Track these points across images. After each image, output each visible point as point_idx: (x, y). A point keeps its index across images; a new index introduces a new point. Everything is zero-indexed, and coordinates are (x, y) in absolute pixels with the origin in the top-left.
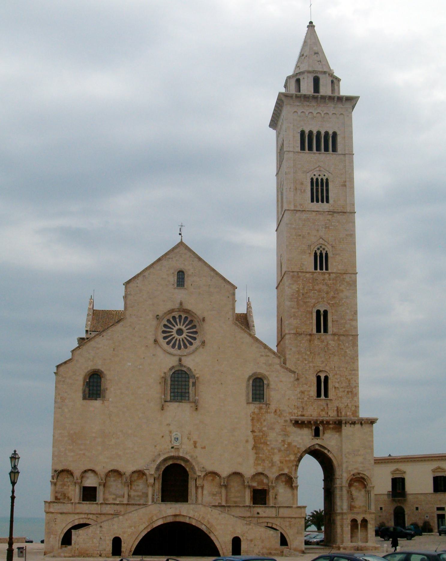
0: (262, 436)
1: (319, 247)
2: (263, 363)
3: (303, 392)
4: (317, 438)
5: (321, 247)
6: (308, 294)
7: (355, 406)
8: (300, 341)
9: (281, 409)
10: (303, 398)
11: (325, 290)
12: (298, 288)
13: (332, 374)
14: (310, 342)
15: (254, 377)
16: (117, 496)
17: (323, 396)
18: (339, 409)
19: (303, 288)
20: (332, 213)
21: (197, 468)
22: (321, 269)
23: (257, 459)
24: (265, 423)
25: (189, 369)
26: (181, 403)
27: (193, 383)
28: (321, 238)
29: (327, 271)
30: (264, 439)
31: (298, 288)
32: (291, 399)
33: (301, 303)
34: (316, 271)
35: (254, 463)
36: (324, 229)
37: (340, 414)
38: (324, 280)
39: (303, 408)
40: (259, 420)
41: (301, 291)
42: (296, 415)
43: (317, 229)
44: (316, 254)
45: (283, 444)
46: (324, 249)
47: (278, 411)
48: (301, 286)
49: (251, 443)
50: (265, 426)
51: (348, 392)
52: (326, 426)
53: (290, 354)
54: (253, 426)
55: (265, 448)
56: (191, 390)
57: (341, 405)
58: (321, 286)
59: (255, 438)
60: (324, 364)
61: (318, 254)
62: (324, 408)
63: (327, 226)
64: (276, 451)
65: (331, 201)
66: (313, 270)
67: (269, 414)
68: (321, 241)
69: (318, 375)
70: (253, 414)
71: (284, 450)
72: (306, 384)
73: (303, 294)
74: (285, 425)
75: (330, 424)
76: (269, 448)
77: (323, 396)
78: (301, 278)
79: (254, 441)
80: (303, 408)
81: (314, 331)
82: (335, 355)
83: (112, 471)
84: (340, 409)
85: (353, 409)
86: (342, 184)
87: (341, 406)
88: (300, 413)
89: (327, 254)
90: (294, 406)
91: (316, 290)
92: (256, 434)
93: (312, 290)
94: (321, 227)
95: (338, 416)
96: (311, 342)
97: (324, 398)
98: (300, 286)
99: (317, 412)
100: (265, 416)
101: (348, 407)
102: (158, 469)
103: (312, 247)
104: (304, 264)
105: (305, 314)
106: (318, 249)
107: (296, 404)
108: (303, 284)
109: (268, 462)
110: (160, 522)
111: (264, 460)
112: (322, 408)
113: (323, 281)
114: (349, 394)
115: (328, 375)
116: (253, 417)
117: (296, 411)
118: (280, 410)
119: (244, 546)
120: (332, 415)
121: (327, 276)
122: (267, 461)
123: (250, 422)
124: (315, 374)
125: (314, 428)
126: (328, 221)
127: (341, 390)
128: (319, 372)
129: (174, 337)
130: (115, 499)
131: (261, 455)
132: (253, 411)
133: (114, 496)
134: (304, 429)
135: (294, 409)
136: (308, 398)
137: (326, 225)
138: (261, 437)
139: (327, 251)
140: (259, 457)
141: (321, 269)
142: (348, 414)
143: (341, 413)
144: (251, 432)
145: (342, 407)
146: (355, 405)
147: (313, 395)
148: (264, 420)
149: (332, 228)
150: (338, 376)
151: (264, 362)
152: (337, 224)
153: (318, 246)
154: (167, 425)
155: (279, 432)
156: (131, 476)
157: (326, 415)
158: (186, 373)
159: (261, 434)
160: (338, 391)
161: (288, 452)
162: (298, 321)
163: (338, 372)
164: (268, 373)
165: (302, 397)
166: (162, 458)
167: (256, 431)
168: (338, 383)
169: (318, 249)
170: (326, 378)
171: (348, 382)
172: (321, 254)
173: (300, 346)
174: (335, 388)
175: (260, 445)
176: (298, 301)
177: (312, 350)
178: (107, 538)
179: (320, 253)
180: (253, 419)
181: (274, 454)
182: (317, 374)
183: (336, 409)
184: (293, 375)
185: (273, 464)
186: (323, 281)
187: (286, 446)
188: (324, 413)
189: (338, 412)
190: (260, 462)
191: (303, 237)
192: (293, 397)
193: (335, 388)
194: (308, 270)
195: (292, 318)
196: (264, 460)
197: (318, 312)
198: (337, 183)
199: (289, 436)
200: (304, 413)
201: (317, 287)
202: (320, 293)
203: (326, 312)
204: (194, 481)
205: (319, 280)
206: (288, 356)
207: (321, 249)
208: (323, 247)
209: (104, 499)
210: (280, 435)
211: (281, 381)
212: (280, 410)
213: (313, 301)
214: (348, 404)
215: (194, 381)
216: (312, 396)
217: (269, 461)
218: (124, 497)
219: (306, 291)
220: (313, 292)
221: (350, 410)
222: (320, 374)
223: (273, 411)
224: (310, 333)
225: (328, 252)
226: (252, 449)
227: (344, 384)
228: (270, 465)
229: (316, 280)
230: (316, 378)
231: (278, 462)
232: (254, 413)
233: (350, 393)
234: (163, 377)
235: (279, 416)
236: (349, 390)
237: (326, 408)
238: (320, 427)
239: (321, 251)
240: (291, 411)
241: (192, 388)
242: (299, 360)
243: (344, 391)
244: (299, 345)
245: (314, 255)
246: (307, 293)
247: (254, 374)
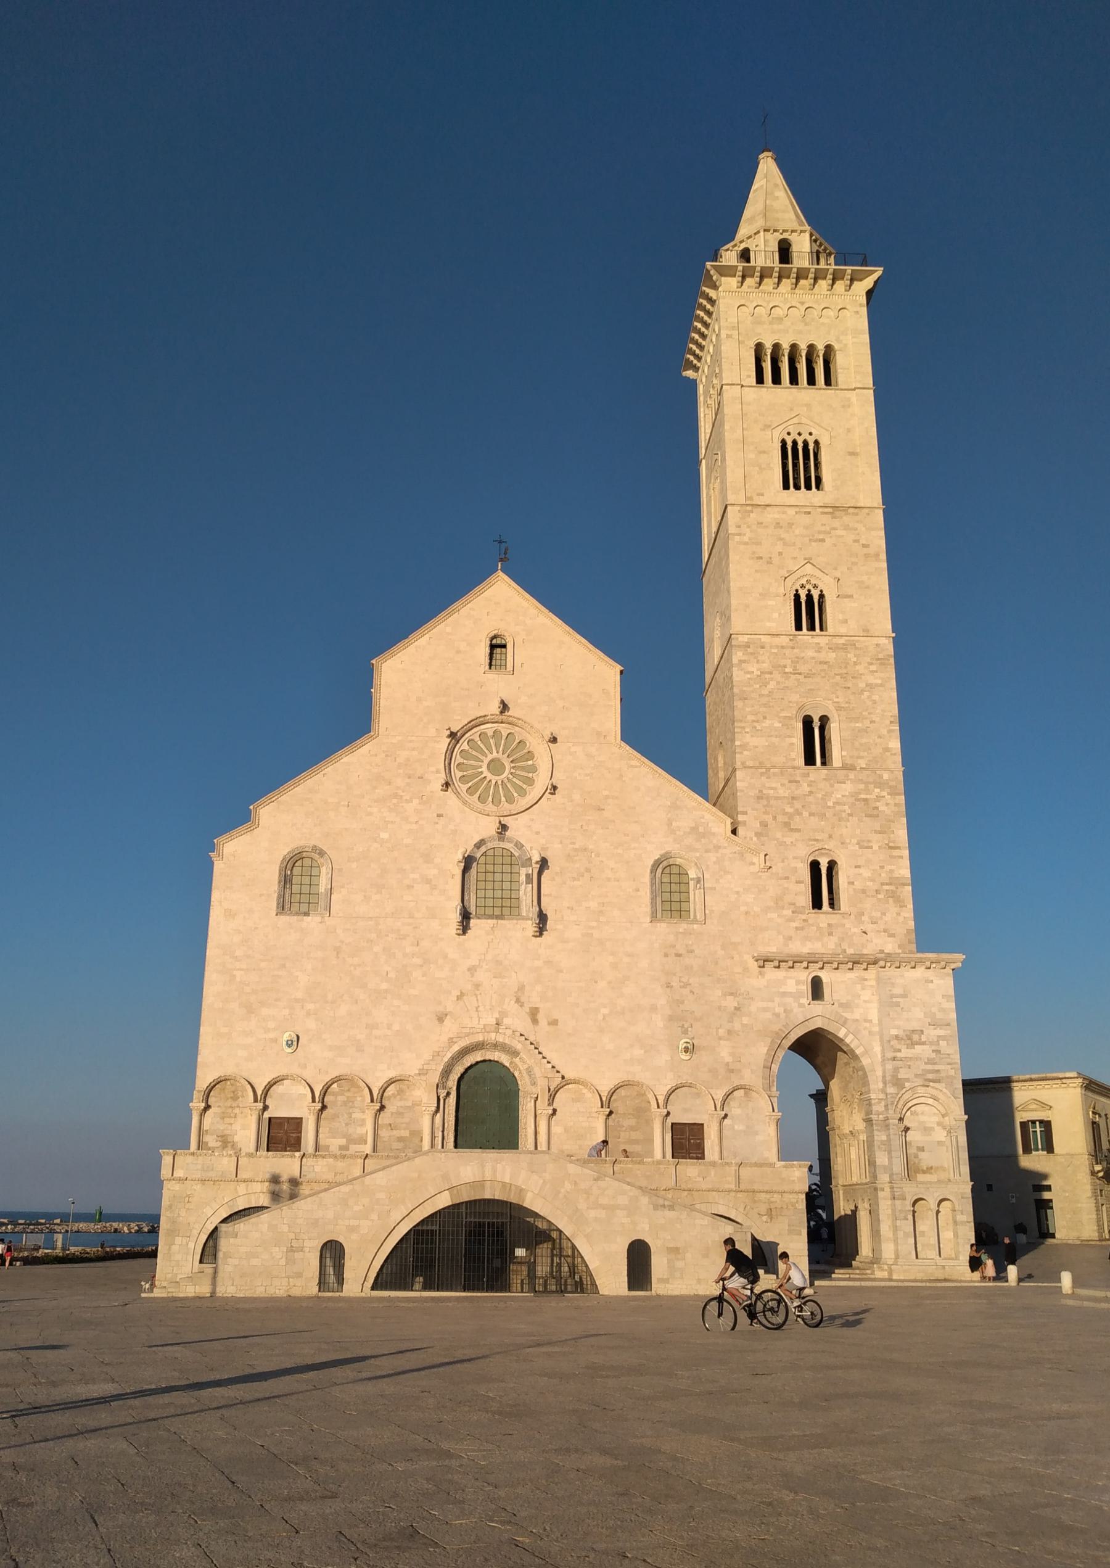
1: (805, 582)
5: (808, 582)
15: (665, 864)
16: (351, 1141)
20: (830, 510)
21: (538, 1072)
22: (812, 628)
25: (519, 846)
26: (500, 921)
27: (528, 876)
29: (822, 633)
34: (800, 633)
44: (797, 597)
46: (815, 586)
56: (526, 893)
61: (803, 599)
81: (801, 760)
83: (337, 1080)
89: (822, 596)
102: (446, 1072)
103: (789, 582)
106: (803, 586)
110: (444, 1201)
119: (658, 1265)
129: (485, 777)
130: (341, 1148)
133: (343, 1142)
139: (821, 591)
141: (812, 628)
153: (804, 581)
154: (469, 970)
156: (384, 1090)
158: (512, 855)
166: (456, 1048)
169: (801, 587)
172: (809, 596)
178: (307, 1244)
184: (755, 860)
191: (770, 562)
204: (533, 1101)
206: (740, 818)
207: (808, 587)
208: (813, 582)
209: (317, 1148)
215: (530, 872)
218: (366, 1143)
225: (824, 593)
234: (460, 862)
239: (809, 591)
241: (526, 888)
245: (794, 600)
247: (666, 856)
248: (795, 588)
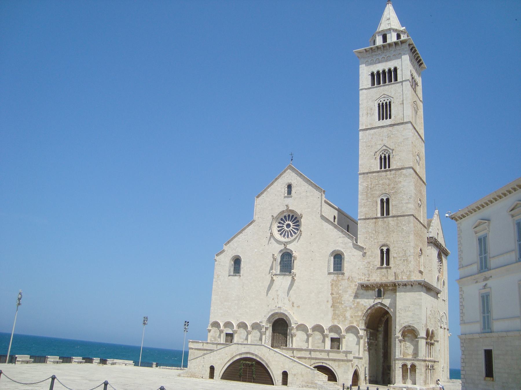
0: (339, 297)
2: (341, 243)
3: (369, 263)
4: (379, 298)
6: (374, 188)
7: (410, 271)
8: (368, 224)
9: (352, 276)
10: (369, 267)
11: (387, 183)
12: (367, 184)
13: (392, 247)
14: (375, 223)
17: (385, 265)
18: (397, 274)
19: (371, 184)
22: (385, 167)
23: (334, 314)
24: (341, 288)
28: (384, 145)
30: (339, 299)
31: (367, 184)
32: (360, 268)
33: (369, 195)
35: (332, 317)
36: (387, 138)
37: (397, 278)
38: (386, 176)
39: (369, 275)
40: (336, 286)
41: (370, 187)
42: (364, 280)
43: (381, 139)
44: (381, 157)
45: (353, 303)
47: (350, 278)
48: (370, 183)
49: (331, 302)
50: (340, 290)
51: (404, 260)
52: (386, 288)
53: (360, 234)
54: (332, 290)
55: (340, 307)
57: (398, 271)
58: (384, 181)
59: (333, 298)
60: (385, 240)
61: (383, 157)
62: (385, 274)
63: (389, 135)
64: (348, 308)
65: (393, 117)
66: (379, 169)
67: (344, 281)
68: (384, 148)
69: (381, 248)
70: (332, 281)
71: (354, 308)
72: (372, 256)
73: (371, 188)
74: (355, 288)
75: (389, 286)
76: (343, 306)
77: (385, 265)
78: (370, 177)
79: (332, 301)
80: (369, 275)
82: (394, 232)
84: (398, 275)
85: (408, 273)
86: (400, 103)
87: (398, 271)
88: (366, 279)
89: (389, 156)
90: (363, 273)
91: (380, 184)
92: (333, 296)
93: (377, 185)
94: (384, 137)
95: (395, 279)
96: (376, 223)
97: (386, 266)
98: (369, 183)
99: (380, 277)
100: (341, 282)
101: (404, 272)
104: (372, 166)
105: (372, 203)
107: (364, 272)
108: (371, 181)
109: (342, 317)
111: (339, 316)
112: (383, 274)
113: (385, 177)
114: (405, 261)
115: (389, 248)
116: (332, 283)
117: (363, 278)
118: (352, 277)
120: (391, 279)
121: (388, 173)
122: (341, 316)
123: (330, 288)
124: (379, 248)
125: (377, 290)
126: (390, 132)
127: (398, 259)
128: (382, 246)
131: (337, 312)
132: (332, 278)
134: (369, 291)
135: (362, 276)
136: (373, 267)
137: (388, 135)
138: (338, 298)
139: (389, 154)
140: (336, 313)
141: (385, 167)
142: (404, 277)
143: (398, 277)
144: (331, 294)
145: (399, 272)
146: (410, 270)
147: (377, 264)
148: (341, 285)
149: (393, 136)
150: (396, 248)
151: (341, 242)
152: (397, 133)
155: (351, 294)
157: (387, 280)
159: (338, 296)
160: (396, 260)
161: (357, 309)
162: (367, 209)
163: (396, 245)
164: (344, 250)
165: (369, 266)
167: (334, 293)
168: (397, 253)
170: (388, 251)
171: (404, 252)
172: (385, 157)
173: (368, 228)
174: (394, 257)
175: (337, 304)
176: (367, 194)
177: (376, 230)
179: (384, 156)
180: (332, 285)
181: (346, 311)
182: (380, 248)
183: (394, 274)
185: (345, 318)
186: (385, 177)
187: (355, 305)
188: (385, 278)
189: (395, 277)
190: (336, 317)
192: (362, 267)
193: (394, 257)
194: (375, 170)
195: (362, 208)
196: (339, 316)
197: (382, 200)
198: (397, 103)
199: (358, 297)
200: (370, 279)
201: (381, 182)
202: (383, 186)
203: (388, 200)
205: (383, 176)
206: (358, 236)
210: (351, 296)
211: (353, 255)
212: (352, 277)
213: (378, 193)
214: (403, 270)
216: (376, 265)
217: (343, 316)
219: (373, 186)
220: (378, 186)
221: (405, 275)
222: (383, 248)
223: (347, 278)
224: (376, 216)
226: (331, 307)
227: (401, 255)
228: (343, 319)
229: (381, 176)
230: (380, 251)
231: (349, 317)
232: (333, 280)
233: (405, 261)
235: (351, 282)
236: (405, 258)
237: (386, 274)
238: (381, 289)
239: (385, 155)
240: (360, 277)
242: (367, 238)
243: (401, 260)
244: (367, 227)
246: (373, 187)
248: (380, 154)
